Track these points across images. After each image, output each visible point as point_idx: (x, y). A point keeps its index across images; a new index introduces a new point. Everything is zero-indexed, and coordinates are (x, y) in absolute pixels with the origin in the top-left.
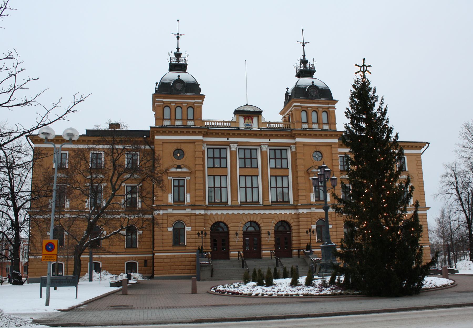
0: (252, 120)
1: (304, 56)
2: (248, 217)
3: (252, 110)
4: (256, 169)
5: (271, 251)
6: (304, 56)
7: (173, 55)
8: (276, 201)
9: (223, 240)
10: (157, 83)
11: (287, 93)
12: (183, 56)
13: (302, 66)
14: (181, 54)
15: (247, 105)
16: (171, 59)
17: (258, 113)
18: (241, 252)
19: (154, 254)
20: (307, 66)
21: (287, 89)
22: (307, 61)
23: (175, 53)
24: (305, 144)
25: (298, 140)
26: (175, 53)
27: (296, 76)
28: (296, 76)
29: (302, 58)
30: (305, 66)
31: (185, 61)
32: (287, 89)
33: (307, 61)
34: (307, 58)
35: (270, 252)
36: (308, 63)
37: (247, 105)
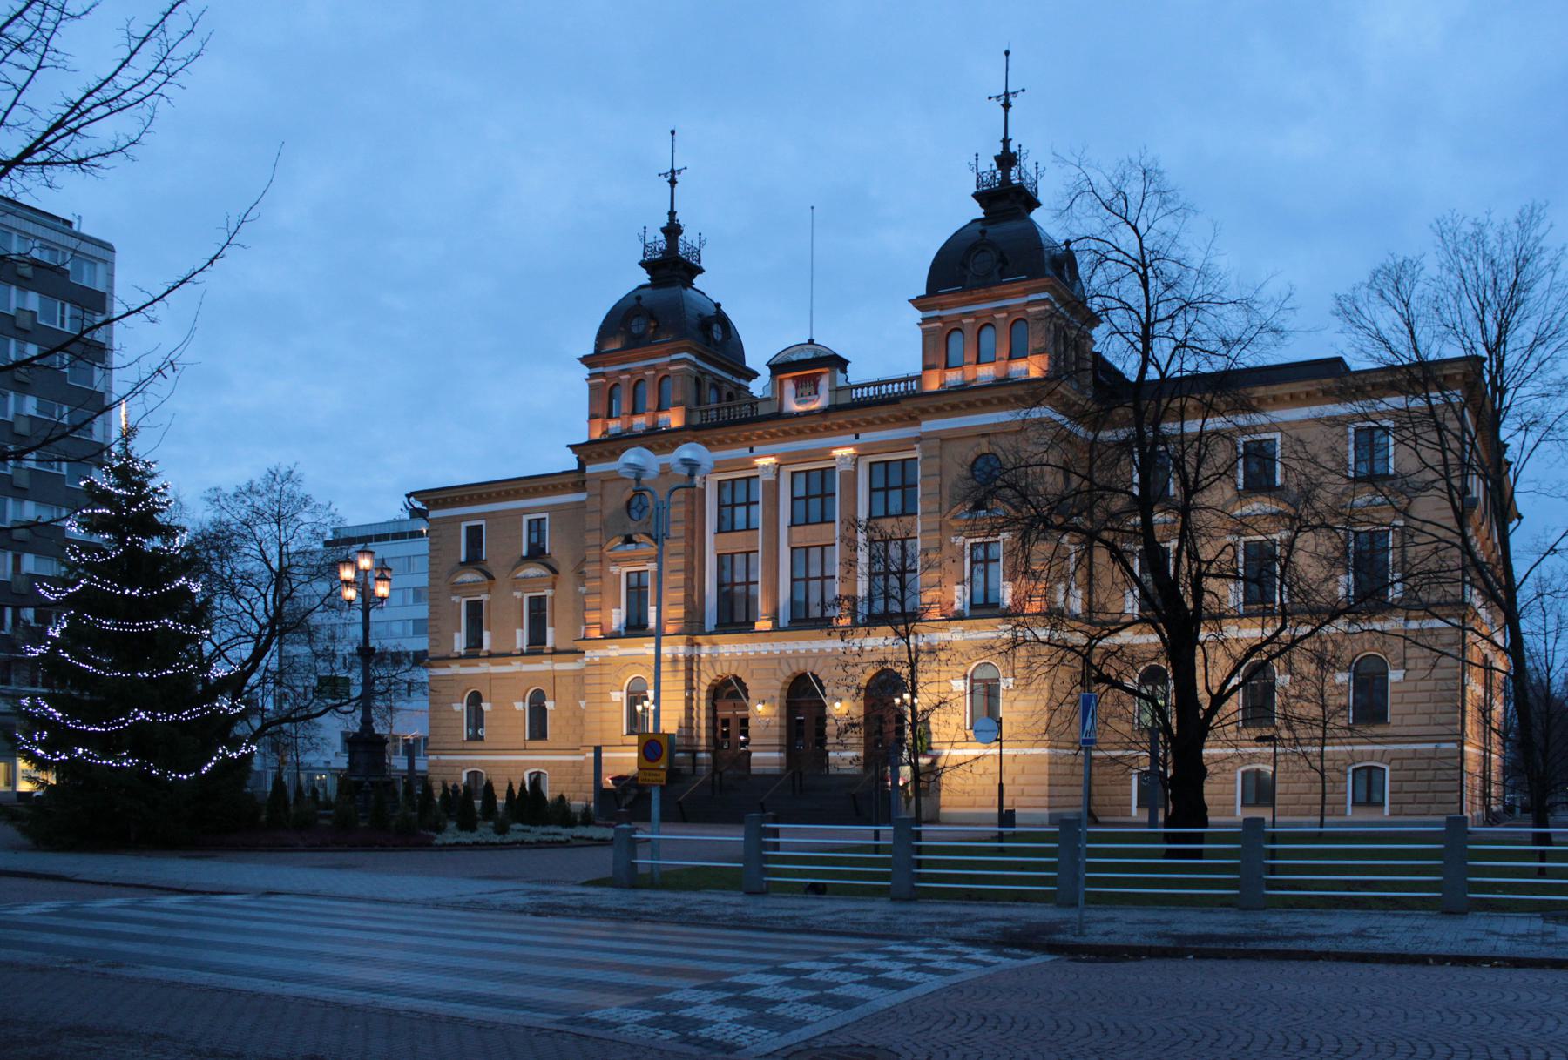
0: (816, 385)
2: (793, 662)
3: (810, 356)
15: (811, 342)
17: (840, 363)
20: (1014, 174)
24: (944, 439)
25: (929, 426)
30: (1006, 175)
37: (811, 342)
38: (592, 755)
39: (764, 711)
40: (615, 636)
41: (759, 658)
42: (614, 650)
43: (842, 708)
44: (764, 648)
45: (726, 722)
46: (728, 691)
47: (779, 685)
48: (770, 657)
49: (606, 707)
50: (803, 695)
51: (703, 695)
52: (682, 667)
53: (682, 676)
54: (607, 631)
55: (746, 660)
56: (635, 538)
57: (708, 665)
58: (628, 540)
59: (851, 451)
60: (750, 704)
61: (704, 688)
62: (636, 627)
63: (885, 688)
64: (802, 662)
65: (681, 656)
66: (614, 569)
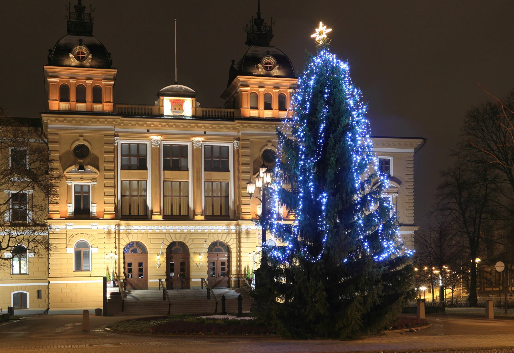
1: (259, 14)
4: (186, 172)
5: (202, 279)
6: (259, 14)
7: (73, 10)
8: (211, 214)
9: (140, 265)
10: (50, 51)
11: (232, 68)
12: (87, 11)
13: (255, 28)
14: (84, 7)
16: (70, 15)
18: (164, 280)
19: (49, 282)
21: (233, 61)
22: (263, 20)
23: (75, 7)
26: (75, 7)
27: (246, 43)
28: (246, 43)
29: (256, 17)
31: (91, 19)
32: (233, 61)
33: (263, 20)
34: (262, 17)
35: (201, 280)
36: (264, 24)
38: (102, 281)
39: (157, 261)
40: (70, 218)
43: (199, 260)
45: (130, 265)
46: (136, 249)
47: (166, 247)
50: (177, 253)
52: (113, 236)
56: (85, 167)
58: (82, 168)
60: (149, 256)
62: (82, 212)
64: (178, 236)
65: (113, 231)
66: (69, 183)
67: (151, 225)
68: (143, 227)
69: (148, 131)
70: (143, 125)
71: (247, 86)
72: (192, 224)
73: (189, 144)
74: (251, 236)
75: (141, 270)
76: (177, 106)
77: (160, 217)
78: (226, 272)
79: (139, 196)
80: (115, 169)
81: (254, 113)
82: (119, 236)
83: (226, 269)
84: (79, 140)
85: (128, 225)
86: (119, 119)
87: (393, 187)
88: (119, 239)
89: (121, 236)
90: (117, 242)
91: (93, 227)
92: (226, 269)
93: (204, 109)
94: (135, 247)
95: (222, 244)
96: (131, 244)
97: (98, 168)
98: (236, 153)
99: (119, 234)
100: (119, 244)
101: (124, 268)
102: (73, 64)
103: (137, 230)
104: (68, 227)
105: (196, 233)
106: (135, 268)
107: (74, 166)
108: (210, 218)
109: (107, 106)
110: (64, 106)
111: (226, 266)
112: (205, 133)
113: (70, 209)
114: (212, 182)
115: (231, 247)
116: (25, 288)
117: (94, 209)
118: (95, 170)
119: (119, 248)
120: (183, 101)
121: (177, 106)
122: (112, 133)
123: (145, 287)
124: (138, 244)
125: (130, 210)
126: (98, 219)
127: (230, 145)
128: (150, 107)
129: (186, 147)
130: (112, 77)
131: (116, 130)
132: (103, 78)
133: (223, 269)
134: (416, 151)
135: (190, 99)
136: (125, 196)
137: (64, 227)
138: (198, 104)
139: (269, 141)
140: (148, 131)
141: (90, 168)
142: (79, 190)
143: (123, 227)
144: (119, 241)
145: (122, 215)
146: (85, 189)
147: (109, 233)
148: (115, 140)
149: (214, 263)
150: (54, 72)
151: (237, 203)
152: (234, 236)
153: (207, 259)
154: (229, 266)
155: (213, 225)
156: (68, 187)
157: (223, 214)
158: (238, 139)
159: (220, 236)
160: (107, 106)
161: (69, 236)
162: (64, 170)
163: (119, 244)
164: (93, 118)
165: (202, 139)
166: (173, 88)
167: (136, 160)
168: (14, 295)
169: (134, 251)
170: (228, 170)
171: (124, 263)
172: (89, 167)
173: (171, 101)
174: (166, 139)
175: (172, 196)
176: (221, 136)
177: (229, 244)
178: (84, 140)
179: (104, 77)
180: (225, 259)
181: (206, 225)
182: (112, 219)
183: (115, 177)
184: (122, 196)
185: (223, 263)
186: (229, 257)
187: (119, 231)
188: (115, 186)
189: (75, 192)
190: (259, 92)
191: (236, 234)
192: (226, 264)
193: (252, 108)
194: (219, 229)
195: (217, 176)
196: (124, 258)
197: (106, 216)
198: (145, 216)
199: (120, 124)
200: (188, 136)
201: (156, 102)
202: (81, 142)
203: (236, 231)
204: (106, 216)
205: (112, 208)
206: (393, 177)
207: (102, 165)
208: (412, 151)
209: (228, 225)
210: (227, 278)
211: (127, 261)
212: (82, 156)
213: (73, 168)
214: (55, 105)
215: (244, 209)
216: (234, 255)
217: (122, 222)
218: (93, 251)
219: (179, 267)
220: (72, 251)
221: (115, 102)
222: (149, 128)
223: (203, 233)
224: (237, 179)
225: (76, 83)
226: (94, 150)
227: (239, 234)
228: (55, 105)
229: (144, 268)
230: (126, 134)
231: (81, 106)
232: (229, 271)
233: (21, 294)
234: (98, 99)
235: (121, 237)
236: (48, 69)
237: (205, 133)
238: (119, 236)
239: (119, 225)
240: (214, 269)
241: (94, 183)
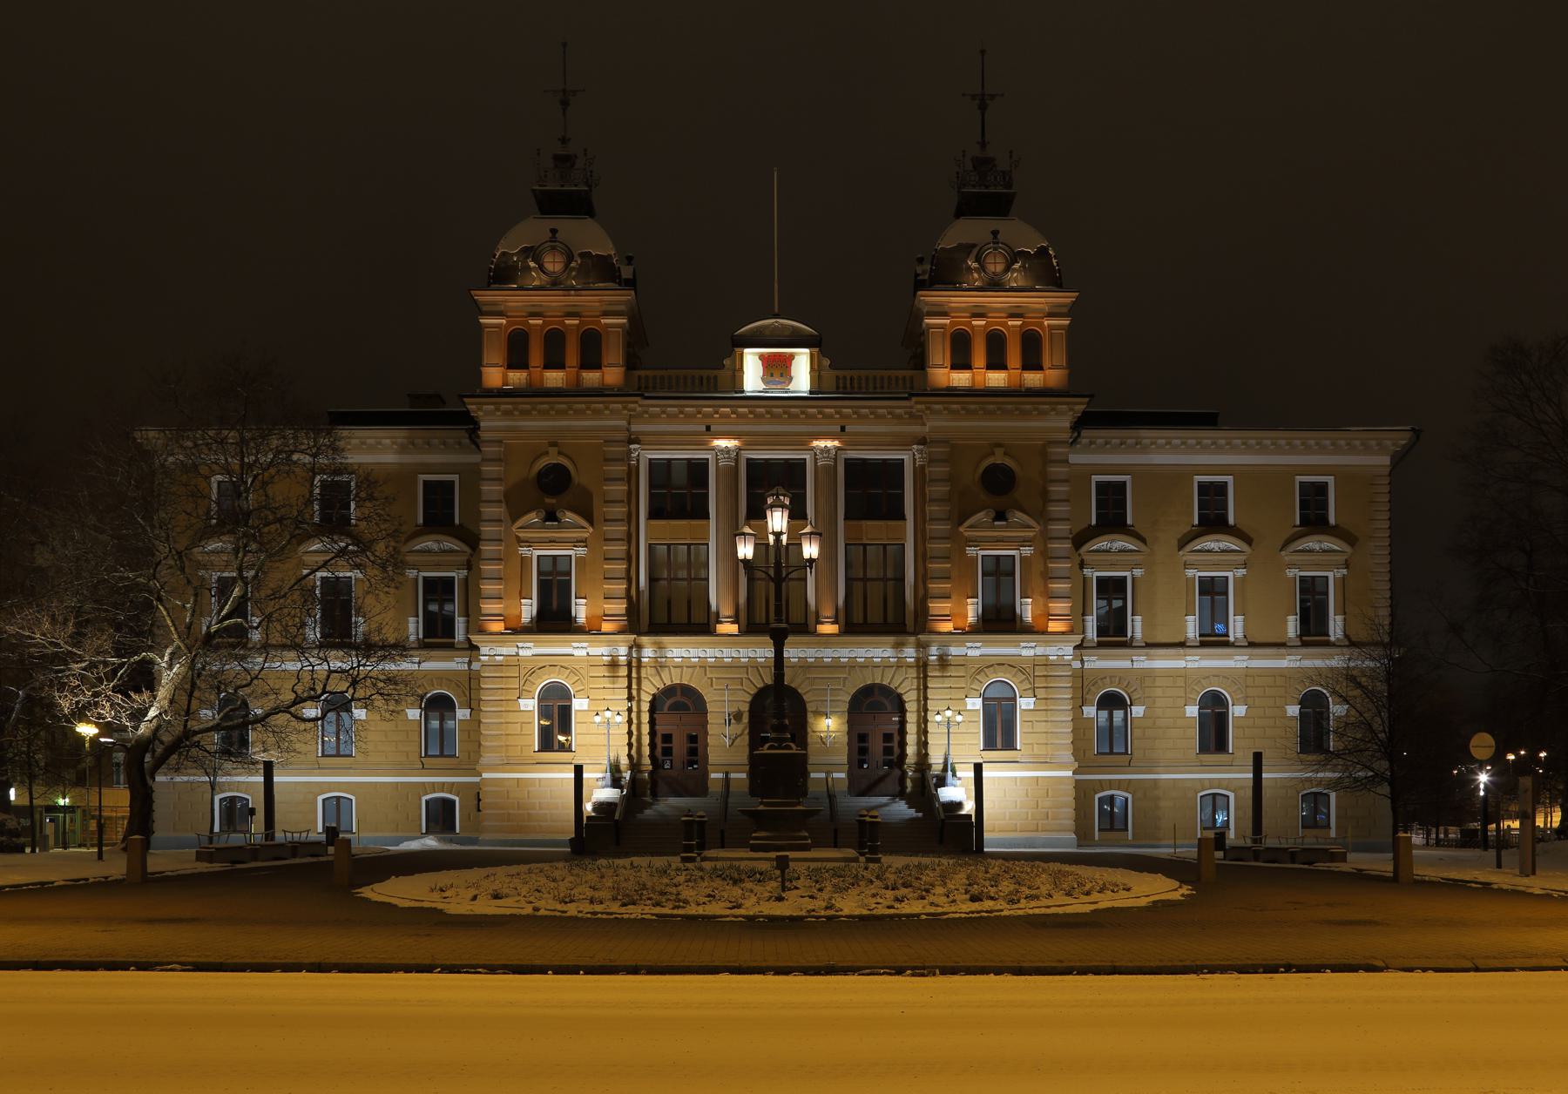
9: (693, 739)
41: (719, 666)
42: (530, 648)
44: (727, 653)
45: (667, 738)
46: (678, 705)
47: (749, 699)
48: (735, 666)
49: (512, 717)
50: (777, 710)
51: (645, 707)
52: (623, 671)
53: (624, 683)
54: (513, 625)
55: (703, 666)
57: (651, 671)
58: (551, 516)
59: (836, 443)
61: (646, 698)
62: (555, 618)
63: (874, 706)
65: (623, 659)
66: (523, 551)
67: (713, 645)
68: (693, 652)
69: (708, 428)
70: (692, 416)
71: (944, 314)
72: (809, 645)
73: (807, 456)
74: (952, 672)
75: (693, 752)
76: (777, 368)
77: (733, 629)
78: (894, 757)
79: (690, 579)
80: (631, 518)
81: (961, 379)
82: (639, 672)
83: (897, 750)
84: (547, 453)
85: (660, 647)
86: (638, 405)
87: (452, 551)
88: (639, 679)
89: (643, 671)
90: (634, 686)
91: (576, 652)
92: (897, 750)
93: (840, 373)
94: (678, 698)
95: (886, 691)
96: (669, 691)
97: (590, 519)
98: (919, 473)
99: (639, 667)
100: (639, 690)
101: (652, 745)
102: (536, 283)
103: (682, 655)
104: (521, 653)
105: (819, 665)
106: (679, 746)
107: (533, 514)
108: (853, 627)
109: (612, 375)
110: (517, 377)
111: (895, 744)
112: (843, 429)
113: (528, 610)
114: (865, 546)
115: (905, 697)
116: (451, 787)
117: (581, 611)
118: (584, 523)
119: (639, 701)
120: (792, 356)
121: (777, 368)
122: (622, 436)
123: (699, 786)
124: (687, 691)
125: (665, 610)
126: (588, 633)
127: (906, 457)
128: (712, 373)
129: (802, 464)
130: (622, 308)
131: (634, 428)
132: (606, 309)
133: (888, 751)
134: (1398, 460)
135: (807, 351)
136: (657, 580)
137: (513, 651)
138: (826, 362)
139: (999, 445)
140: (708, 428)
141: (569, 517)
142: (548, 567)
143: (648, 653)
144: (639, 684)
145: (650, 624)
146: (561, 567)
147: (613, 665)
148: (630, 452)
149: (863, 738)
150: (494, 303)
151: (921, 592)
152: (913, 673)
153: (845, 728)
154: (903, 744)
155: (861, 645)
156: (525, 562)
157: (890, 619)
158: (922, 441)
159: (878, 672)
160: (612, 375)
161: (523, 672)
162: (514, 521)
163: (639, 690)
164: (543, 404)
165: (836, 443)
166: (766, 327)
167: (680, 494)
168: (427, 802)
169: (676, 707)
170: (903, 518)
171: (652, 733)
172: (569, 514)
173: (761, 357)
174: (749, 445)
175: (865, 580)
176: (885, 436)
177: (900, 691)
178: (560, 453)
179: (605, 308)
180: (894, 729)
181: (844, 645)
182: (619, 633)
183: (631, 538)
184: (652, 580)
185: (888, 737)
186: (903, 723)
187: (639, 660)
188: (631, 559)
189: (540, 573)
190: (973, 327)
191: (918, 667)
192: (896, 738)
193: (954, 367)
194: (876, 654)
195: (874, 531)
196: (652, 722)
197: (606, 627)
198: (700, 625)
199: (640, 416)
200: (802, 441)
201: (727, 362)
202: (553, 458)
203: (917, 659)
204: (606, 627)
205: (620, 607)
206: (1337, 526)
207: (599, 509)
208: (1385, 460)
209: (898, 646)
210: (897, 772)
211: (661, 729)
212: (554, 491)
213: (533, 518)
214: (493, 376)
215: (936, 607)
216: (911, 718)
217: (645, 640)
218: (578, 704)
219: (686, 745)
220: (530, 704)
221: (631, 364)
222: (708, 421)
223: (836, 666)
224: (921, 537)
225: (542, 327)
226: (580, 477)
227: (922, 666)
228: (493, 376)
229: (699, 745)
230: (660, 440)
231: (554, 378)
232: (903, 755)
233: (444, 800)
234: (591, 359)
235: (643, 675)
236: (485, 297)
237: (843, 429)
238: (639, 672)
239: (639, 647)
240: (863, 751)
241: (581, 551)
